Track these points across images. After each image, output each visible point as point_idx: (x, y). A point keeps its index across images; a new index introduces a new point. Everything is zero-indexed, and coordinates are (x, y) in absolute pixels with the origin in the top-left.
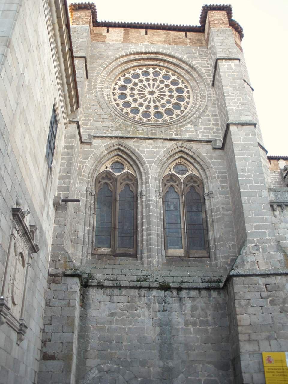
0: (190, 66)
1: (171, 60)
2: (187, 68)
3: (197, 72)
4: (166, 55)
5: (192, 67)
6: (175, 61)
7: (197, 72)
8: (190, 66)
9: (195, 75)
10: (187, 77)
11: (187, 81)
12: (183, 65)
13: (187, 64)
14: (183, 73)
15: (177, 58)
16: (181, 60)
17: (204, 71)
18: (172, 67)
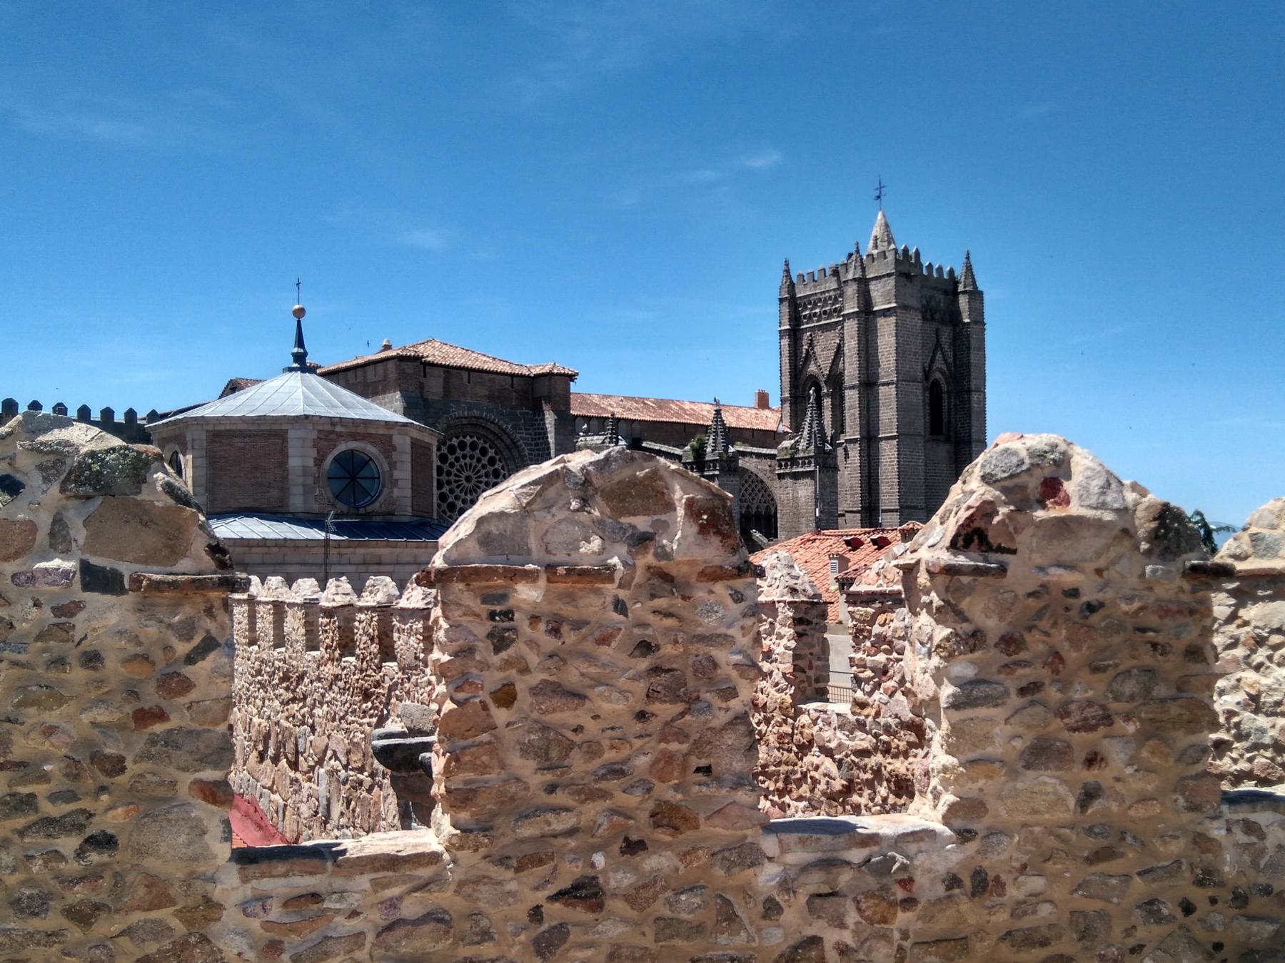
0: (512, 440)
1: (492, 427)
2: (508, 442)
3: (519, 452)
4: (488, 421)
5: (514, 443)
6: (496, 430)
7: (519, 452)
8: (512, 440)
9: (516, 454)
10: (507, 454)
11: (506, 461)
12: (505, 437)
13: (509, 436)
14: (502, 447)
15: (500, 427)
16: (504, 430)
17: (527, 452)
18: (491, 436)
